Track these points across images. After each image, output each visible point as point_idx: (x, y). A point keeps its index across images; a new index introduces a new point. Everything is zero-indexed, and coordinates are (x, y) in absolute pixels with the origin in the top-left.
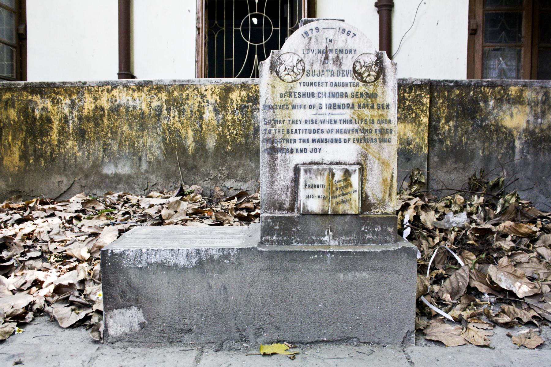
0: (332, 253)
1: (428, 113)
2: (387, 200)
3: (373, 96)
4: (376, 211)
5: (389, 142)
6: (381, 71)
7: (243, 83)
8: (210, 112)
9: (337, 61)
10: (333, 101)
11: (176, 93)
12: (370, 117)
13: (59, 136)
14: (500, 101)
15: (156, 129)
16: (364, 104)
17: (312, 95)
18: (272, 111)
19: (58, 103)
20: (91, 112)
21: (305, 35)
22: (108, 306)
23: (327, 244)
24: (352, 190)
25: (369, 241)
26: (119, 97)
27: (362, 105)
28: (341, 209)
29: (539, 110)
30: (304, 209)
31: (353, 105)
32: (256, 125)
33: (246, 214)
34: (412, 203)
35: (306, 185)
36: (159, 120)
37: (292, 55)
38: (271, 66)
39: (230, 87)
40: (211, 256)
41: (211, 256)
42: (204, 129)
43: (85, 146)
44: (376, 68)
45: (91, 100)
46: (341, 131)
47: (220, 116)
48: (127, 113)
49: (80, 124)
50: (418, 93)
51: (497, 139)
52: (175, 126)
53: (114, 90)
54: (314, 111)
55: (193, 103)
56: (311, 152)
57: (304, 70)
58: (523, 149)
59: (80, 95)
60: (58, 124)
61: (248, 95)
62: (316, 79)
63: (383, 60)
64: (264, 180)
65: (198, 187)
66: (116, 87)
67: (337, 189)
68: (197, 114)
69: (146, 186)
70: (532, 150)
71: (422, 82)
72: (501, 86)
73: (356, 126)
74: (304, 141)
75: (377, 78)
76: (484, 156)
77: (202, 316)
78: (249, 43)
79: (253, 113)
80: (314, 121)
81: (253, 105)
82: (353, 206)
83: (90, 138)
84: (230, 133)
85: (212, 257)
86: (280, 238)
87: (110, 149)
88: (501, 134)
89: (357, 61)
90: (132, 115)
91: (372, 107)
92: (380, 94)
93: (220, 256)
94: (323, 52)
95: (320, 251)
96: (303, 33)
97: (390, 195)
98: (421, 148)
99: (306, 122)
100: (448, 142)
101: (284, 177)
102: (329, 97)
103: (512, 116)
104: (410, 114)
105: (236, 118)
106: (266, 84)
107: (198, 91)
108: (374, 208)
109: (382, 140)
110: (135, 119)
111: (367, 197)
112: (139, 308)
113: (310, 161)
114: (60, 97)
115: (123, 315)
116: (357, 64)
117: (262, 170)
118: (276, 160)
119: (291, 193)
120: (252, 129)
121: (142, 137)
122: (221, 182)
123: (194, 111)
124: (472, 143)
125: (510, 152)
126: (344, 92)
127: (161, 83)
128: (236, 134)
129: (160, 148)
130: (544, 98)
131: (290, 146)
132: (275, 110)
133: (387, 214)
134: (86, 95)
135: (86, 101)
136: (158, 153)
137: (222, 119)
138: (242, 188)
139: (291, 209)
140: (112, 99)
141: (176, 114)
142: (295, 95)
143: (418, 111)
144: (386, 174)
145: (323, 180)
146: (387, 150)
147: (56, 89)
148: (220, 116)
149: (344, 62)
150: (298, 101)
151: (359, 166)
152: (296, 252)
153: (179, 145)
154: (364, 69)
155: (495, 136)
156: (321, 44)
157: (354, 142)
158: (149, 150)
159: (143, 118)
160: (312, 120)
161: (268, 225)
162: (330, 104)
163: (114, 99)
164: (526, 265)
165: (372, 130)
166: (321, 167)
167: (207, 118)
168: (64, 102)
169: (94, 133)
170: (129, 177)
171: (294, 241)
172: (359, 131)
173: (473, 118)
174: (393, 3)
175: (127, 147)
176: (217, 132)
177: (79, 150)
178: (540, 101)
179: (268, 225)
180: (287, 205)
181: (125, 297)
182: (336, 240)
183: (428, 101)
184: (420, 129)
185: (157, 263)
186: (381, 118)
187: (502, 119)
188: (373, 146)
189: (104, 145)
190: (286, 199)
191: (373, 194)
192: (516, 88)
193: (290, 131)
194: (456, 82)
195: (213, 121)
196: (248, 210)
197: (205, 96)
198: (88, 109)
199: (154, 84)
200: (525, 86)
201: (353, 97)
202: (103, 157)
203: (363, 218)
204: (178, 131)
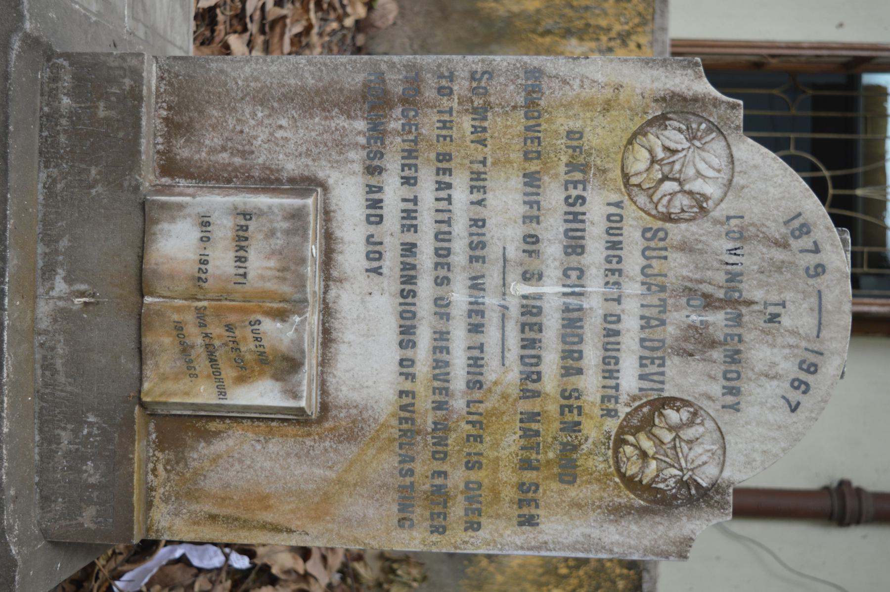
2: (195, 507)
3: (568, 469)
4: (160, 467)
5: (402, 522)
6: (656, 502)
9: (698, 342)
10: (552, 323)
12: (492, 454)
16: (537, 433)
17: (575, 245)
18: (520, 100)
21: (796, 223)
23: (41, 290)
24: (228, 382)
25: (49, 440)
27: (534, 426)
28: (160, 341)
30: (164, 206)
35: (246, 215)
37: (724, 176)
38: (685, 99)
42: (540, 40)
44: (672, 482)
54: (513, 253)
56: (369, 239)
57: (668, 218)
62: (633, 262)
63: (699, 508)
64: (273, 68)
67: (229, 328)
68: (579, 24)
73: (459, 404)
75: (631, 483)
80: (478, 253)
86: (64, 121)
89: (695, 414)
91: (526, 465)
92: (573, 492)
94: (735, 290)
97: (213, 518)
99: (478, 223)
102: (567, 309)
108: (168, 462)
111: (208, 436)
113: (338, 233)
116: (685, 415)
118: (342, 112)
119: (225, 167)
123: (588, 15)
131: (393, 164)
133: (149, 505)
139: (170, 167)
142: (575, 184)
144: (287, 507)
145: (262, 277)
146: (371, 512)
149: (696, 367)
150: (554, 196)
151: (313, 411)
154: (667, 437)
156: (761, 285)
157: (402, 393)
160: (483, 245)
162: (540, 309)
165: (443, 459)
171: (55, 172)
172: (439, 413)
180: (183, 151)
182: (55, 320)
186: (484, 492)
188: (387, 463)
190: (206, 147)
191: (219, 456)
193: (445, 165)
197: (624, 44)
201: (566, 395)
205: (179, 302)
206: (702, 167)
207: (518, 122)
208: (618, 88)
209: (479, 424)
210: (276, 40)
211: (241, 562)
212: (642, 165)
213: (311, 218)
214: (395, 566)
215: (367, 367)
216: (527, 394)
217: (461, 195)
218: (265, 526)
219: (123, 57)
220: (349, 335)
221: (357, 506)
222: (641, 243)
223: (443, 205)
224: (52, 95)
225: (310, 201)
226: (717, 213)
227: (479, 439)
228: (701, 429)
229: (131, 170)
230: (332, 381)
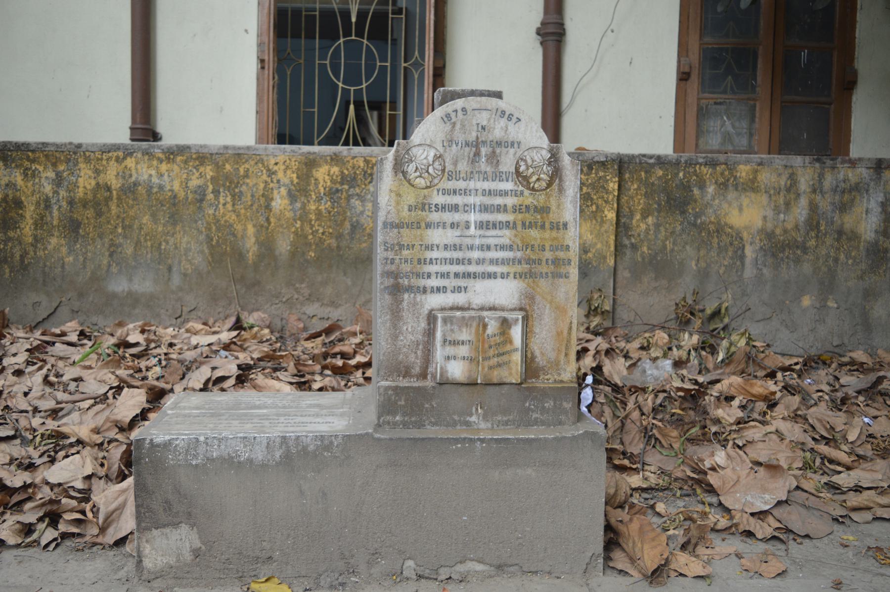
0: (482, 441)
1: (615, 205)
2: (562, 362)
3: (544, 210)
4: (546, 377)
5: (567, 277)
7: (335, 154)
8: (282, 198)
9: (493, 158)
10: (486, 217)
11: (228, 167)
12: (539, 241)
13: (36, 229)
14: (723, 186)
15: (196, 222)
16: (530, 223)
17: (455, 208)
18: (396, 230)
19: (33, 176)
21: (446, 119)
24: (512, 348)
25: (536, 422)
26: (136, 169)
27: (527, 224)
29: (781, 201)
30: (441, 375)
31: (515, 223)
33: (340, 362)
34: (592, 346)
35: (445, 341)
36: (200, 208)
37: (427, 148)
39: (314, 160)
40: (303, 447)
45: (90, 173)
46: (497, 262)
47: (298, 205)
48: (149, 196)
49: (71, 211)
50: (601, 174)
51: (718, 244)
52: (227, 217)
54: (458, 233)
55: (257, 182)
56: (453, 292)
57: (443, 171)
59: (71, 164)
60: (34, 211)
61: (342, 172)
62: (461, 184)
65: (263, 316)
66: (131, 154)
67: (490, 347)
68: (262, 200)
69: (179, 311)
70: (770, 260)
71: (607, 157)
72: (726, 164)
73: (519, 254)
75: (549, 185)
76: (699, 271)
77: (289, 535)
78: (341, 85)
79: (349, 201)
81: (350, 188)
82: (514, 372)
83: (88, 234)
85: (305, 448)
88: (724, 237)
89: (522, 159)
90: (157, 200)
91: (543, 227)
92: (553, 208)
93: (318, 447)
95: (465, 439)
97: (566, 355)
98: (605, 258)
99: (446, 247)
100: (645, 249)
101: (413, 328)
102: (480, 211)
103: (741, 209)
104: (588, 206)
105: (322, 207)
107: (263, 164)
109: (557, 275)
110: (162, 205)
111: (533, 358)
112: (192, 526)
113: (450, 305)
114: (38, 167)
115: (167, 538)
116: (522, 163)
117: (380, 317)
121: (173, 234)
122: (298, 307)
123: (257, 195)
124: (680, 251)
125: (738, 263)
126: (502, 204)
127: (205, 151)
128: (323, 233)
129: (202, 252)
130: (789, 182)
131: (422, 282)
133: (562, 382)
134: (82, 166)
135: (82, 174)
136: (198, 260)
137: (301, 208)
139: (423, 375)
141: (229, 199)
142: (430, 208)
143: (600, 202)
145: (470, 334)
146: (563, 290)
147: (30, 154)
148: (298, 205)
149: (503, 159)
150: (435, 217)
153: (233, 249)
154: (531, 170)
155: (716, 240)
156: (470, 133)
159: (174, 205)
161: (389, 400)
162: (481, 222)
163: (128, 173)
164: (760, 445)
166: (467, 314)
167: (278, 207)
168: (44, 175)
169: (95, 227)
170: (152, 297)
171: (427, 422)
173: (683, 212)
174: (564, 30)
175: (149, 250)
176: (293, 229)
177: (69, 253)
178: (782, 187)
179: (389, 400)
180: (417, 370)
181: (170, 509)
183: (616, 187)
184: (603, 229)
186: (555, 243)
187: (726, 214)
188: (542, 282)
189: (111, 246)
190: (415, 361)
192: (748, 167)
194: (659, 158)
195: (287, 213)
196: (344, 355)
197: (275, 173)
198: (85, 187)
199: (193, 151)
200: (760, 164)
201: (515, 211)
202: (109, 266)
203: (528, 389)
204: (231, 226)
205: (480, 369)
206: (423, 157)
207: (405, 231)
208: (391, 191)
209: (527, 246)
210: (307, 369)
211: (589, 379)
212: (422, 181)
214: (593, 308)
215: (504, 292)
216: (515, 226)
217: (434, 254)
219: (380, 395)
221: (561, 295)
222: (454, 181)
223: (439, 262)
225: (439, 315)
226: (441, 150)
227: (533, 246)
229: (426, 390)
230: (510, 307)
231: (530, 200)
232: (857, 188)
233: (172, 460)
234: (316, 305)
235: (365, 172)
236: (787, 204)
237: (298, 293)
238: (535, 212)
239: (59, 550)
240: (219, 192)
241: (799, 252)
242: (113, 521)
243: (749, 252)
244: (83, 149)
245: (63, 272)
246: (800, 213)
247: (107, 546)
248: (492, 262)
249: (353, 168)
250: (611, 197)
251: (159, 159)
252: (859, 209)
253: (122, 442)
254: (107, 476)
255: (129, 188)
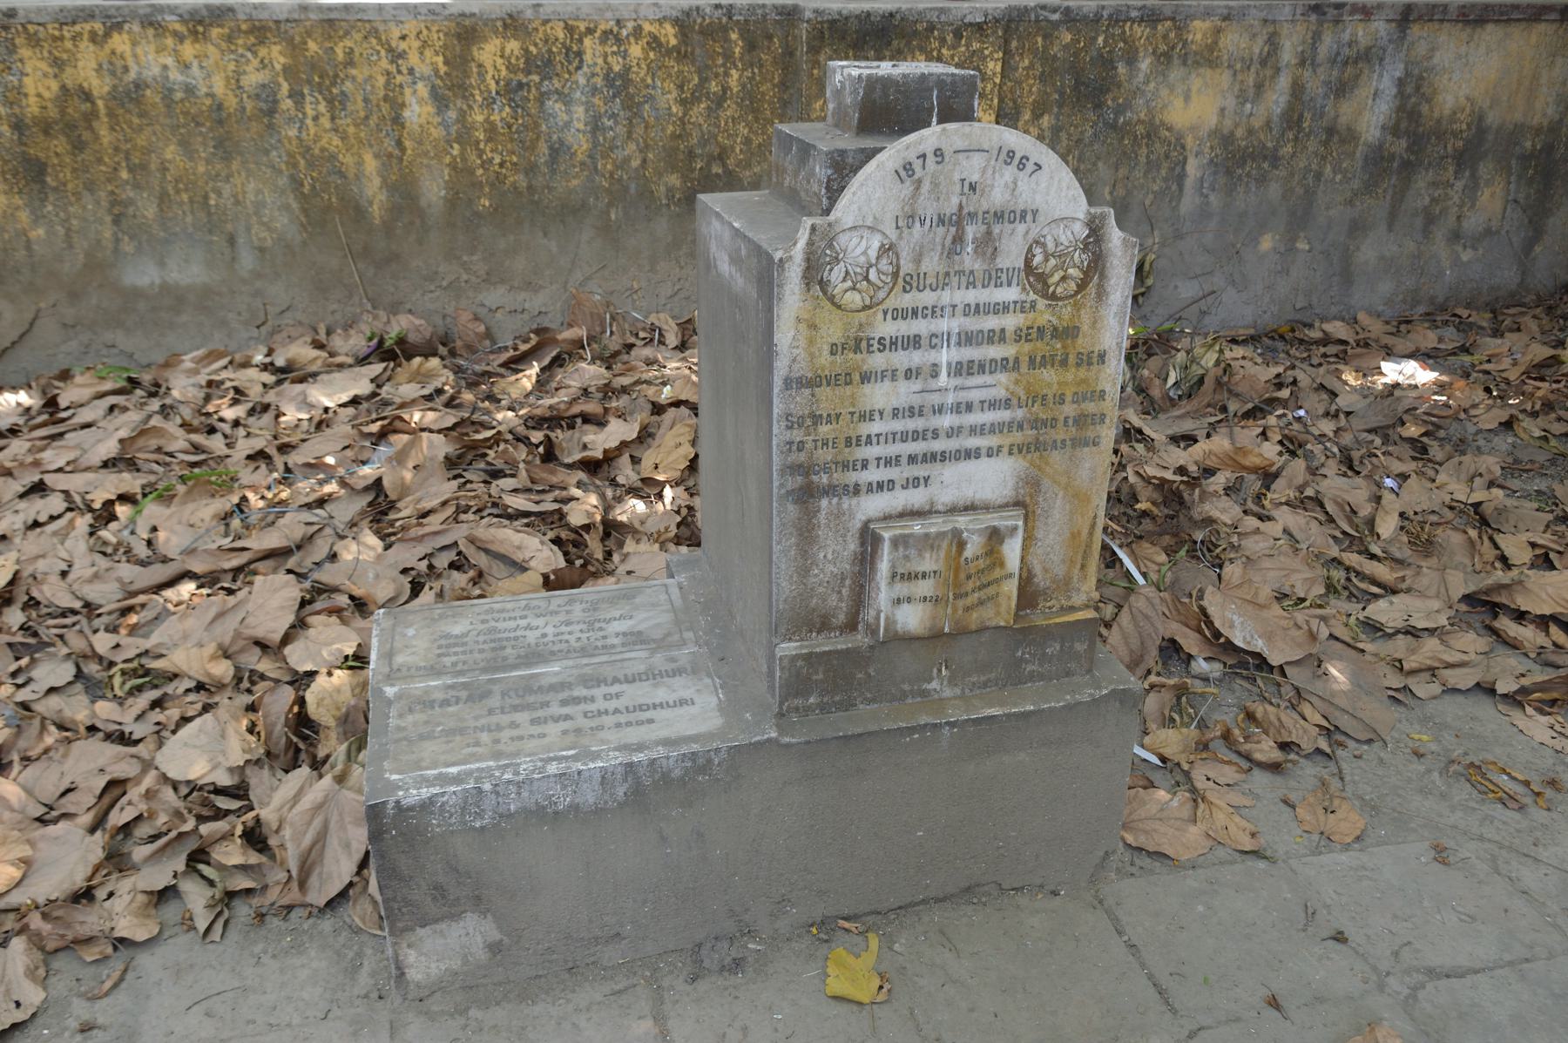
0: (952, 725)
3: (1068, 333)
7: (511, 16)
8: (421, 102)
9: (988, 246)
11: (312, 46)
12: (1055, 387)
14: (1164, 59)
15: (267, 152)
16: (1043, 357)
17: (914, 342)
18: (807, 392)
20: (49, 105)
21: (903, 173)
22: (400, 925)
24: (1003, 573)
25: (1032, 677)
26: (135, 56)
28: (974, 619)
29: (1251, 81)
32: (555, 137)
35: (894, 576)
36: (270, 126)
37: (866, 233)
38: (808, 268)
39: (474, 29)
40: (663, 774)
41: (663, 774)
42: (409, 152)
43: (50, 208)
45: (44, 66)
47: (452, 115)
48: (168, 106)
50: (976, 45)
51: (1148, 157)
52: (324, 142)
53: (116, 36)
54: (917, 385)
55: (370, 75)
57: (895, 275)
58: (1202, 180)
61: (527, 51)
62: (927, 298)
65: (417, 322)
66: (118, 27)
67: (969, 577)
68: (385, 108)
69: (262, 315)
70: (1222, 180)
72: (1173, 19)
73: (1020, 414)
74: (888, 462)
75: (1082, 286)
79: (542, 103)
83: (65, 185)
84: (483, 162)
85: (666, 776)
87: (134, 216)
88: (1158, 145)
89: (1037, 242)
90: (186, 114)
92: (1085, 328)
95: (926, 725)
96: (898, 165)
97: (1083, 567)
99: (896, 413)
101: (835, 552)
102: (959, 344)
103: (1187, 98)
105: (496, 117)
106: (792, 320)
107: (379, 38)
109: (1078, 443)
110: (198, 124)
112: (484, 914)
113: (900, 509)
116: (1038, 250)
120: (543, 148)
125: (1174, 187)
127: (264, 15)
128: (501, 165)
129: (287, 207)
131: (853, 477)
132: (817, 390)
135: (28, 69)
136: (282, 222)
137: (458, 121)
138: (527, 306)
140: (111, 63)
141: (322, 108)
142: (869, 346)
146: (1087, 465)
148: (452, 115)
152: (870, 734)
154: (1052, 262)
155: (1144, 151)
156: (948, 199)
158: (256, 214)
159: (220, 122)
163: (119, 63)
164: (1267, 563)
167: (415, 119)
169: (74, 170)
173: (1098, 106)
175: (186, 208)
176: (448, 160)
180: (842, 617)
181: (443, 897)
183: (999, 69)
185: (526, 813)
187: (1165, 106)
188: (1056, 457)
189: (114, 203)
192: (1208, 24)
197: (402, 55)
198: (39, 95)
199: (242, 17)
200: (1226, 18)
202: (117, 240)
204: (333, 157)
206: (859, 251)
207: (824, 392)
208: (799, 320)
213: (898, 532)
215: (991, 478)
217: (876, 427)
218: (1091, 534)
220: (969, 493)
221: (1084, 473)
222: (914, 292)
223: (882, 439)
224: (808, 710)
225: (886, 535)
226: (893, 234)
227: (1044, 397)
228: (1049, 237)
230: (1000, 501)
231: (1047, 316)
232: (1368, 57)
233: (439, 826)
234: (502, 290)
235: (568, 49)
236: (1259, 87)
237: (467, 270)
238: (1053, 337)
239: (233, 934)
240: (303, 96)
241: (1266, 165)
242: (314, 863)
243: (1193, 168)
244: (21, 18)
245: (31, 256)
246: (1277, 102)
247: (315, 911)
248: (974, 430)
249: (546, 41)
250: (989, 87)
251: (175, 34)
252: (1363, 92)
253: (277, 681)
254: (268, 754)
255: (128, 93)
